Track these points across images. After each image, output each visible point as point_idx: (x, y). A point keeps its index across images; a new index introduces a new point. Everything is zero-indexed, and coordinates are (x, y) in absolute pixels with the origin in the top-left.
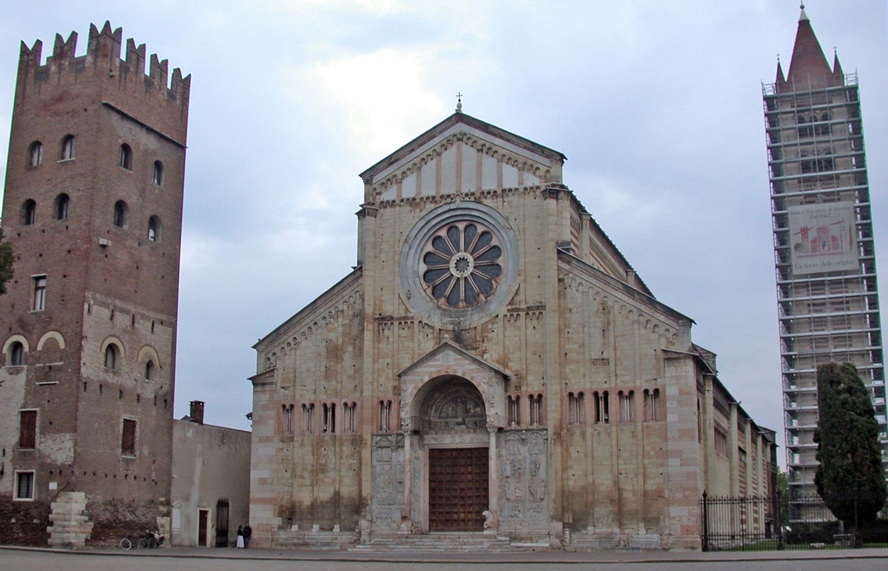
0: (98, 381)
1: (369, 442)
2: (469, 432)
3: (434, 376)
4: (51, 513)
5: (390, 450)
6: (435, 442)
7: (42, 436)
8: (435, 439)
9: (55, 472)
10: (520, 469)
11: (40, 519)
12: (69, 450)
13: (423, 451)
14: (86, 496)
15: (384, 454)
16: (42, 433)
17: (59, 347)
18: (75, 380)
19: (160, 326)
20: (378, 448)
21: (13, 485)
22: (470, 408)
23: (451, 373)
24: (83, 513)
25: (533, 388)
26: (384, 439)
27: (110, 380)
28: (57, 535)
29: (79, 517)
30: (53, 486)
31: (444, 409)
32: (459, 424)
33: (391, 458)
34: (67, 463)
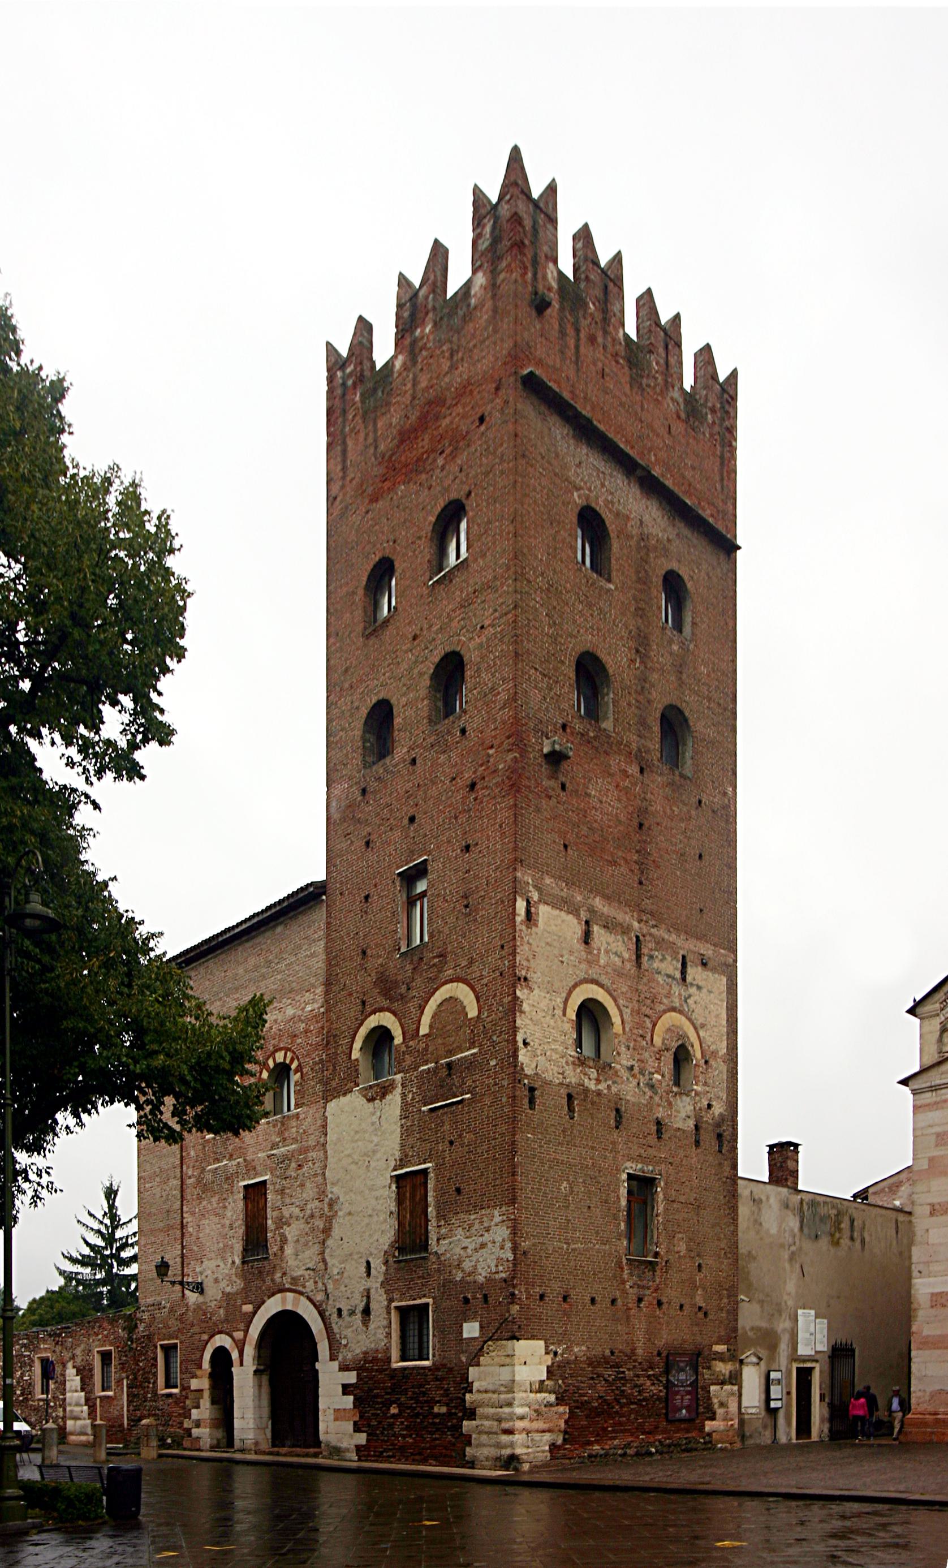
0: (561, 1084)
4: (471, 1392)
7: (442, 1223)
9: (475, 1298)
11: (447, 1405)
12: (502, 1248)
14: (547, 1347)
16: (440, 1216)
17: (467, 1014)
18: (505, 1083)
19: (700, 968)
21: (389, 1335)
24: (541, 1388)
27: (592, 1085)
28: (484, 1438)
29: (532, 1395)
30: (471, 1330)
34: (497, 1276)
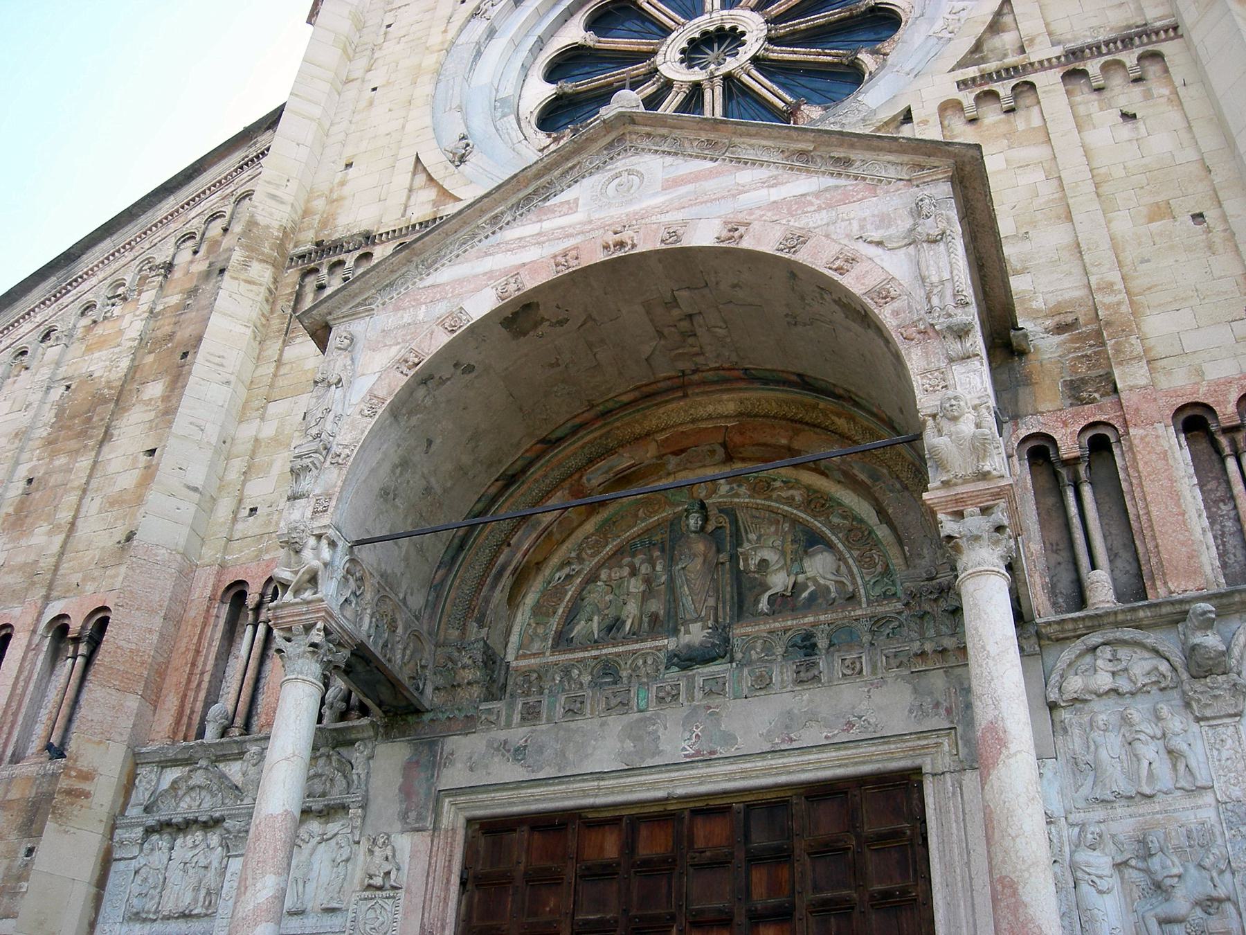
1: (104, 793)
2: (763, 684)
3: (530, 284)
5: (214, 839)
6: (514, 772)
8: (519, 753)
10: (1210, 904)
13: (423, 840)
15: (175, 874)
20: (149, 831)
22: (764, 563)
23: (647, 243)
25: (1200, 373)
26: (199, 778)
31: (598, 594)
32: (688, 660)
33: (213, 894)
